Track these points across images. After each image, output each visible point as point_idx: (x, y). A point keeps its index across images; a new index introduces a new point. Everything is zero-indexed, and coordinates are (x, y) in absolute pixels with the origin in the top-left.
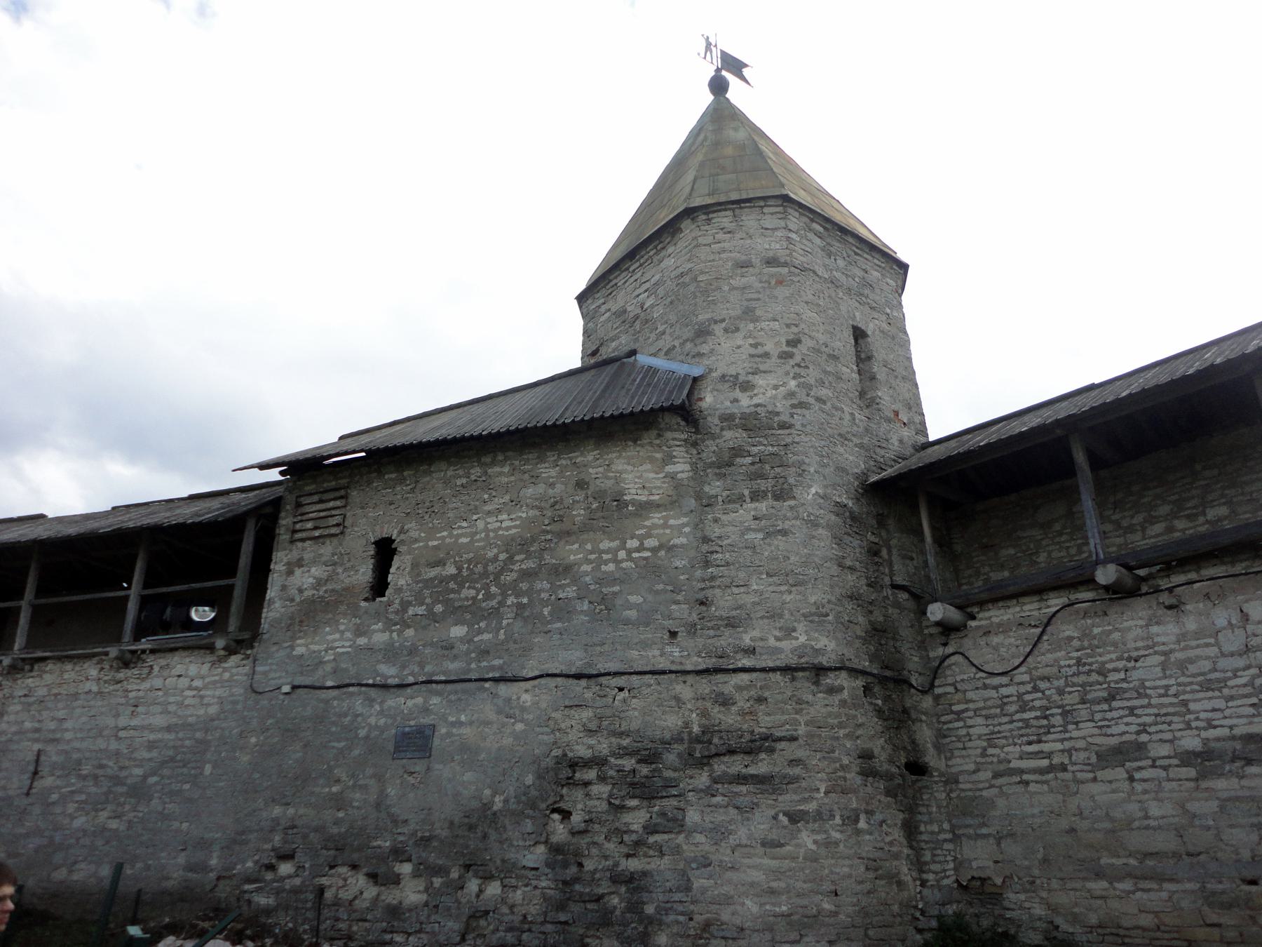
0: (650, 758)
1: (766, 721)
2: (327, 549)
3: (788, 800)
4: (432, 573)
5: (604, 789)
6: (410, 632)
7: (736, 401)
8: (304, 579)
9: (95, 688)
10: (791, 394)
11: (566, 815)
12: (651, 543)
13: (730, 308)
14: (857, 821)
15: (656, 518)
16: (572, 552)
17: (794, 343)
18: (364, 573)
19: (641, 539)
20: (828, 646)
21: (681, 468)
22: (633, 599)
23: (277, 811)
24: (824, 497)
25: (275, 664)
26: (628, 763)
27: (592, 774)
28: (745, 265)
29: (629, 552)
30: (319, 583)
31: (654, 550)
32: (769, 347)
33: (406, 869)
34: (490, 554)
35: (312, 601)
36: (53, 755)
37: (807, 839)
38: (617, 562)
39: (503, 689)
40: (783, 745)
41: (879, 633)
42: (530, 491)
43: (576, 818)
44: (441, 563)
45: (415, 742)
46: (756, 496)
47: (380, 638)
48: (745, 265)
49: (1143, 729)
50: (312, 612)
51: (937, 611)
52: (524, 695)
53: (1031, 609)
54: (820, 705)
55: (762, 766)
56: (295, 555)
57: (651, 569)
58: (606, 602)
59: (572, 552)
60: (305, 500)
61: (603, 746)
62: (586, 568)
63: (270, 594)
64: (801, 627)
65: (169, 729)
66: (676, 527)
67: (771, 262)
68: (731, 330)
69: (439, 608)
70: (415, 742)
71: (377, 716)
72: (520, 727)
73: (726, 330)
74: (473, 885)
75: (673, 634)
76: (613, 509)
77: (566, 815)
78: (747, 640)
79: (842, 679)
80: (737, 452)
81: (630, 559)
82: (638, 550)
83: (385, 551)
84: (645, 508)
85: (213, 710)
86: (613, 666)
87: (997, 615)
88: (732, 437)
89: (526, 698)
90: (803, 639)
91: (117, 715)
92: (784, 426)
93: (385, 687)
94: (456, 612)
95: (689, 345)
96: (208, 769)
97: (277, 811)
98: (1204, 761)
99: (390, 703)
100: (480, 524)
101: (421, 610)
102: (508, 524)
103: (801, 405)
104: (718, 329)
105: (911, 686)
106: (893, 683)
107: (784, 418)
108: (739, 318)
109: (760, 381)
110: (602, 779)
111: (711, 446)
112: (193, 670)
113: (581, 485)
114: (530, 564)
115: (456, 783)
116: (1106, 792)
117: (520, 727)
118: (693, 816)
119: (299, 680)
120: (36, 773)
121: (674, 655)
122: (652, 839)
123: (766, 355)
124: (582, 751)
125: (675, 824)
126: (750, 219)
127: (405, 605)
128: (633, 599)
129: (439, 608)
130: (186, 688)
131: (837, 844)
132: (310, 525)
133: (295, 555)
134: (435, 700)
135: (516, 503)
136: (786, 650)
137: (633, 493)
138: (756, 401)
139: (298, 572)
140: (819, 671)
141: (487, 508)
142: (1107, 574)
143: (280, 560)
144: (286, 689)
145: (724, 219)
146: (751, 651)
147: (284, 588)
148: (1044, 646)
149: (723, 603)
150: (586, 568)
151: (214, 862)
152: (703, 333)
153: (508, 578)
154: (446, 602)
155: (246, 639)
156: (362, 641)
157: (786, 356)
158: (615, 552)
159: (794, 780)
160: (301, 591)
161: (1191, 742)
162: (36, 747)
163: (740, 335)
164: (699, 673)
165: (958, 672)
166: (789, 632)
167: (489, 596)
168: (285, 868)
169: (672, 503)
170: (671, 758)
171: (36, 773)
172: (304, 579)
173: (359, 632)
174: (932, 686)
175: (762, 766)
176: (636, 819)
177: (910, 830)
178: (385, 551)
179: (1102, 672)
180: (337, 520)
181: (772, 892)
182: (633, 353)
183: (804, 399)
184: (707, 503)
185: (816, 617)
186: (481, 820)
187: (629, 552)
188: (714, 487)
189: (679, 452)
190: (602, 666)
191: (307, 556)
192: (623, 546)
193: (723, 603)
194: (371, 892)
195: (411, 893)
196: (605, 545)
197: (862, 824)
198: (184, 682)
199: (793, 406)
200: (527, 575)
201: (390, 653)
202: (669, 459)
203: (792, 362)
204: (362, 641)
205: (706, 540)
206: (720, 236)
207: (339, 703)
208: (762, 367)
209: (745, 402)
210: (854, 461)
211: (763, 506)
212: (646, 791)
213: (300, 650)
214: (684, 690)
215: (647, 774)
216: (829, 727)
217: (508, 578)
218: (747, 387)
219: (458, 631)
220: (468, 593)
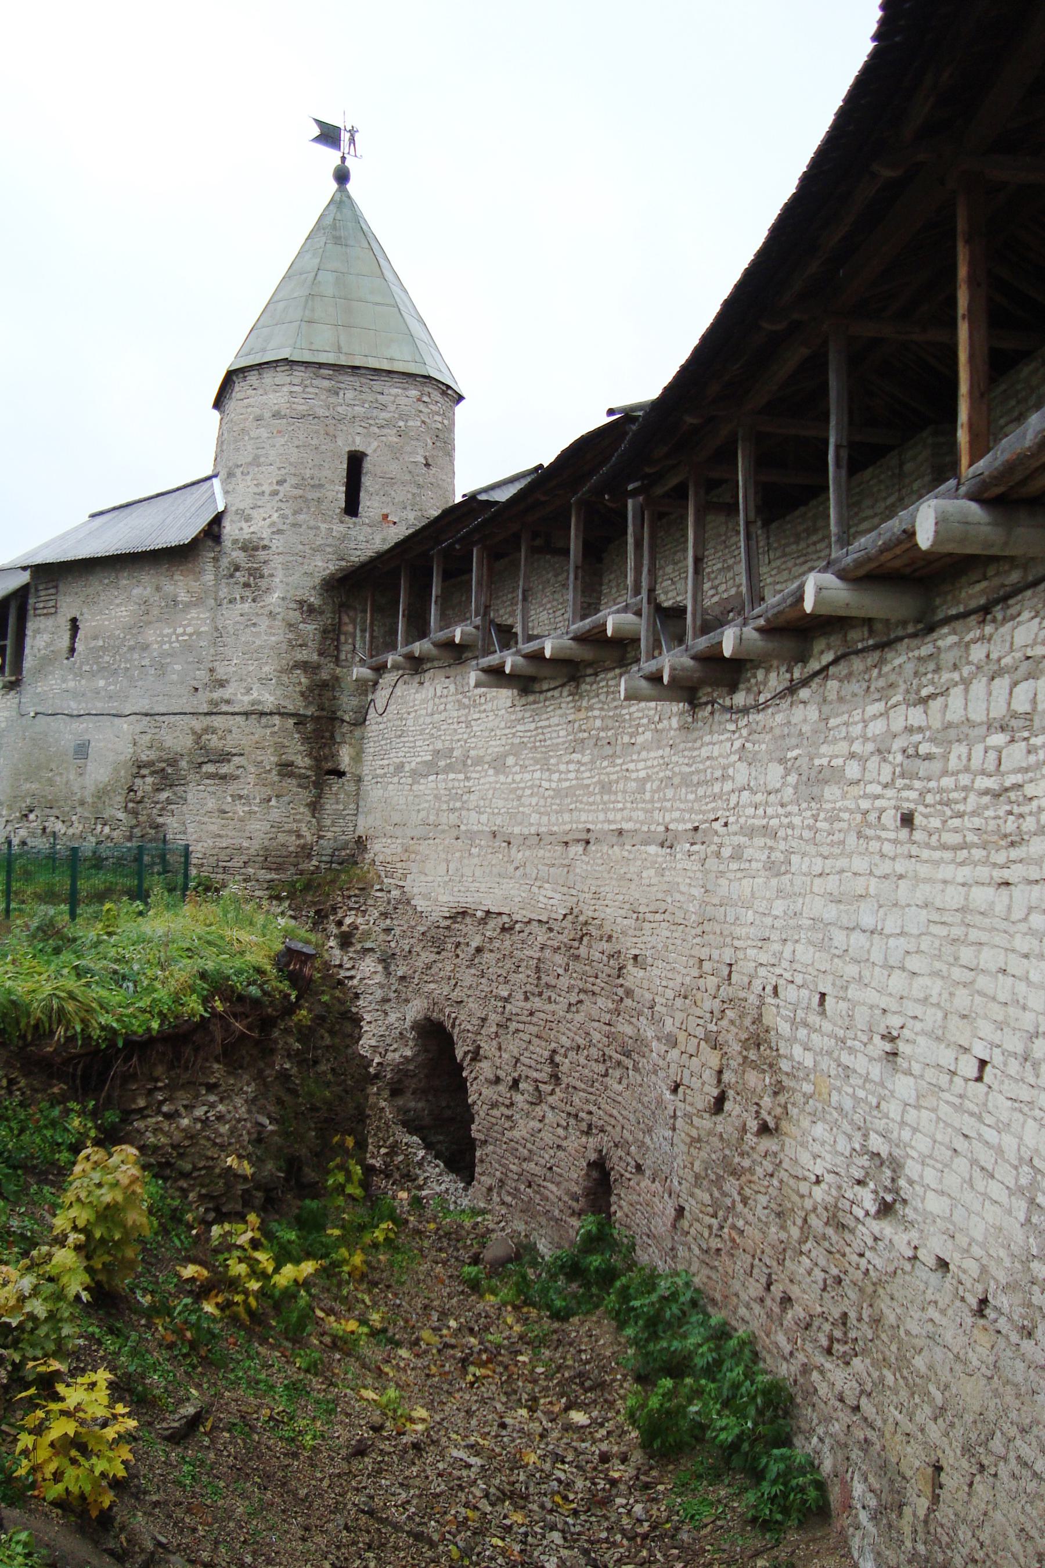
0: (173, 762)
1: (229, 744)
3: (233, 788)
4: (93, 644)
5: (149, 780)
6: (83, 682)
7: (241, 529)
10: (273, 524)
12: (189, 630)
14: (269, 800)
16: (150, 635)
17: (280, 483)
18: (65, 642)
19: (185, 627)
20: (269, 699)
21: (209, 577)
22: (178, 667)
24: (283, 599)
29: (178, 636)
30: (48, 645)
31: (191, 635)
35: (43, 658)
37: (241, 810)
38: (171, 643)
40: (235, 758)
42: (135, 592)
44: (95, 638)
45: (82, 751)
47: (71, 684)
52: (124, 725)
55: (224, 769)
58: (162, 669)
63: (27, 651)
64: (255, 687)
67: (276, 415)
74: (99, 827)
79: (276, 720)
81: (178, 641)
82: (184, 634)
83: (74, 625)
86: (163, 710)
89: (125, 726)
90: (255, 695)
92: (265, 547)
98: (414, 773)
99: (74, 726)
103: (279, 532)
104: (238, 471)
105: (343, 721)
107: (266, 542)
108: (250, 464)
109: (254, 513)
110: (153, 773)
111: (225, 562)
114: (132, 643)
115: (98, 773)
118: (190, 796)
119: (39, 710)
122: (170, 807)
124: (144, 758)
127: (82, 663)
128: (178, 667)
131: (255, 813)
132: (41, 605)
133: (35, 626)
136: (244, 701)
137: (183, 597)
138: (252, 530)
140: (262, 714)
141: (117, 601)
143: (31, 626)
145: (253, 378)
146: (228, 702)
148: (392, 701)
149: (221, 672)
150: (156, 646)
154: (97, 663)
156: (64, 686)
157: (275, 493)
158: (169, 635)
159: (237, 778)
163: (249, 478)
164: (206, 714)
165: (372, 714)
170: (183, 764)
173: (64, 681)
174: (365, 720)
175: (224, 769)
177: (315, 807)
178: (74, 625)
180: (52, 603)
181: (220, 836)
183: (281, 527)
185: (264, 681)
186: (102, 794)
187: (178, 636)
189: (209, 567)
190: (156, 710)
191: (42, 626)
196: (167, 631)
197: (273, 803)
199: (273, 533)
200: (132, 649)
201: (76, 695)
203: (277, 498)
204: (64, 686)
205: (217, 629)
206: (251, 392)
208: (259, 503)
210: (324, 566)
213: (39, 690)
216: (261, 748)
219: (102, 683)
220: (107, 658)
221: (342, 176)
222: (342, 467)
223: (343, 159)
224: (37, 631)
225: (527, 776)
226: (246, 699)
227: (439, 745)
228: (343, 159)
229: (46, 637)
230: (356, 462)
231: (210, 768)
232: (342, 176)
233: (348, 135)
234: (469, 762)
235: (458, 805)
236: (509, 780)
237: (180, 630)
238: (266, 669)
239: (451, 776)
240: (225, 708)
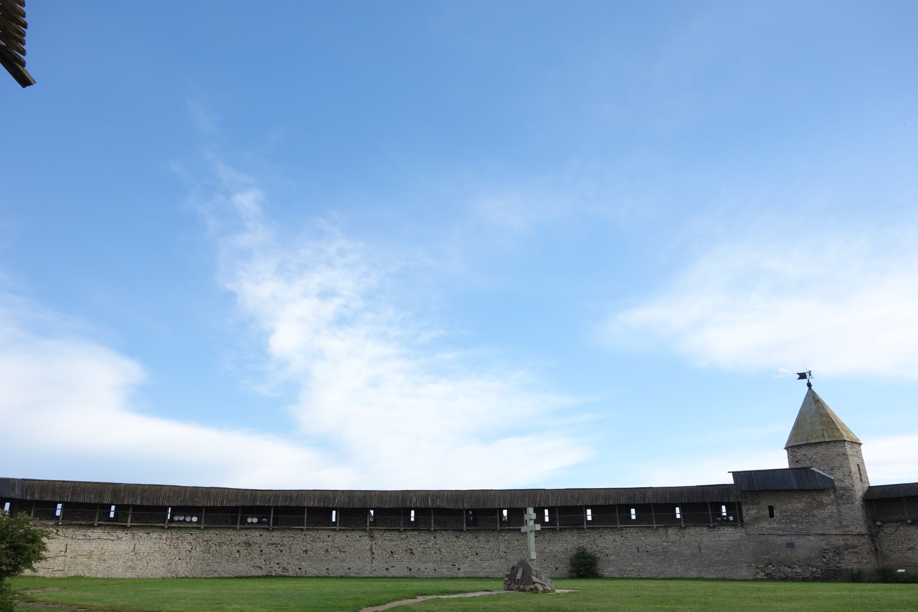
1: (855, 543)
2: (756, 507)
8: (753, 512)
13: (838, 464)
16: (815, 512)
18: (767, 512)
20: (864, 531)
21: (833, 497)
25: (750, 529)
36: (702, 546)
41: (869, 527)
50: (756, 520)
51: (878, 523)
53: (895, 524)
54: (864, 541)
56: (748, 507)
57: (831, 516)
58: (824, 522)
59: (815, 512)
61: (829, 547)
66: (833, 509)
70: (791, 545)
71: (781, 541)
83: (771, 509)
87: (889, 524)
88: (841, 492)
94: (792, 522)
106: (873, 536)
111: (838, 494)
116: (909, 554)
121: (837, 532)
125: (843, 559)
126: (838, 444)
130: (729, 535)
135: (801, 502)
137: (825, 502)
140: (862, 535)
142: (909, 521)
143: (744, 508)
149: (845, 523)
152: (832, 469)
155: (743, 524)
165: (881, 533)
169: (832, 504)
172: (753, 512)
176: (837, 558)
178: (771, 509)
184: (839, 504)
193: (845, 523)
207: (770, 538)
209: (843, 485)
212: (839, 554)
214: (840, 538)
215: (838, 551)
216: (864, 545)
221: (809, 385)
224: (748, 510)
231: (851, 550)
232: (809, 385)
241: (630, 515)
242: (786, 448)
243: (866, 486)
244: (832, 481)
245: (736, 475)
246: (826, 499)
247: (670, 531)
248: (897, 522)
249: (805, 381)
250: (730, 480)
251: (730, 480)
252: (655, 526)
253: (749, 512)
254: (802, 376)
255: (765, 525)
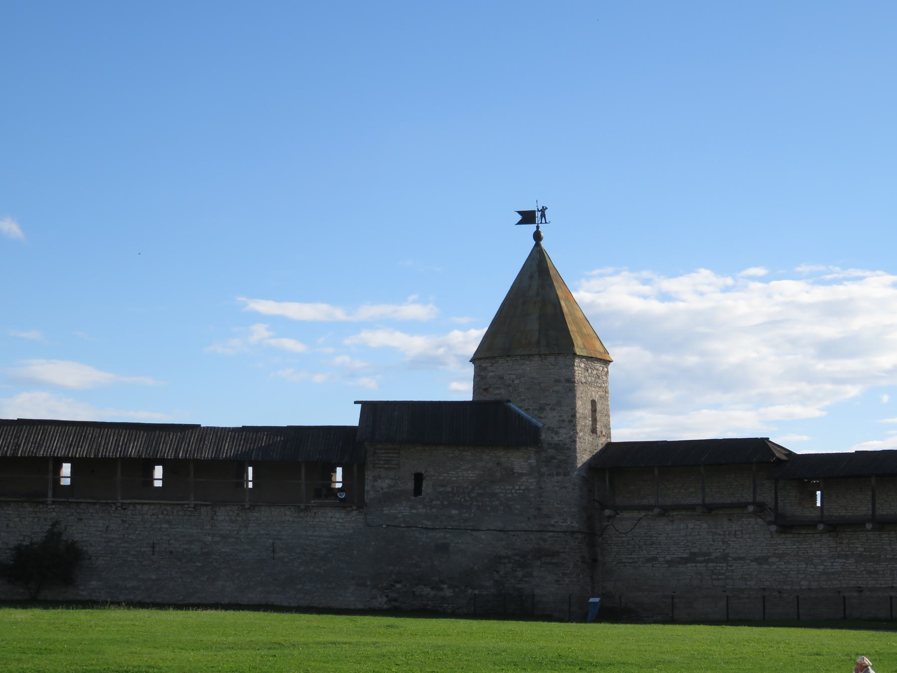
4: (441, 489)
5: (511, 565)
6: (434, 510)
9: (291, 519)
11: (498, 572)
15: (524, 479)
18: (411, 485)
21: (533, 461)
22: (518, 507)
23: (391, 568)
26: (517, 558)
27: (506, 561)
28: (558, 381)
30: (390, 487)
32: (565, 417)
33: (445, 586)
34: (465, 485)
37: (567, 580)
39: (474, 533)
43: (502, 573)
46: (558, 474)
47: (422, 511)
48: (558, 381)
49: (658, 553)
53: (635, 514)
55: (555, 561)
60: (378, 451)
62: (502, 495)
65: (332, 537)
68: (552, 409)
69: (446, 503)
70: (443, 548)
72: (481, 546)
73: (551, 409)
75: (529, 519)
76: (510, 475)
77: (498, 572)
78: (552, 522)
79: (579, 535)
80: (553, 458)
82: (519, 489)
83: (419, 479)
84: (521, 475)
85: (351, 531)
87: (626, 515)
88: (551, 452)
91: (306, 531)
93: (426, 528)
95: (536, 412)
96: (355, 552)
97: (391, 568)
98: (670, 563)
100: (460, 474)
101: (439, 503)
102: (472, 475)
104: (548, 408)
106: (592, 535)
109: (562, 431)
112: (337, 515)
113: (499, 464)
117: (481, 546)
118: (535, 573)
120: (273, 551)
123: (563, 421)
128: (518, 507)
129: (446, 503)
130: (335, 523)
134: (448, 535)
137: (517, 469)
139: (379, 481)
140: (573, 532)
143: (369, 475)
144: (384, 526)
146: (554, 526)
147: (373, 486)
150: (502, 495)
151: (369, 583)
152: (542, 409)
153: (473, 495)
155: (361, 505)
160: (382, 489)
161: (668, 558)
162: (271, 541)
166: (565, 521)
167: (465, 500)
168: (398, 586)
171: (273, 551)
172: (384, 484)
173: (412, 508)
176: (520, 573)
178: (419, 479)
179: (651, 537)
182: (509, 401)
188: (544, 469)
192: (514, 488)
194: (432, 593)
195: (448, 593)
196: (508, 487)
198: (334, 520)
202: (529, 458)
204: (414, 511)
205: (541, 488)
211: (560, 478)
213: (386, 512)
217: (473, 495)
218: (557, 433)
219: (454, 512)
221: (537, 236)
222: (589, 407)
223: (538, 227)
224: (375, 479)
225: (792, 566)
226: (564, 524)
227: (696, 550)
228: (538, 227)
229: (388, 481)
230: (593, 403)
232: (537, 236)
233: (540, 213)
234: (730, 559)
235: (723, 577)
236: (775, 567)
237: (517, 487)
238: (573, 510)
239: (710, 564)
240: (551, 529)
241: (151, 479)
242: (473, 360)
243: (603, 441)
244: (536, 430)
245: (370, 409)
246: (520, 461)
247: (222, 514)
248: (639, 508)
249: (532, 228)
250: (351, 418)
251: (351, 418)
252: (192, 503)
253: (377, 483)
254: (527, 217)
255: (402, 510)
